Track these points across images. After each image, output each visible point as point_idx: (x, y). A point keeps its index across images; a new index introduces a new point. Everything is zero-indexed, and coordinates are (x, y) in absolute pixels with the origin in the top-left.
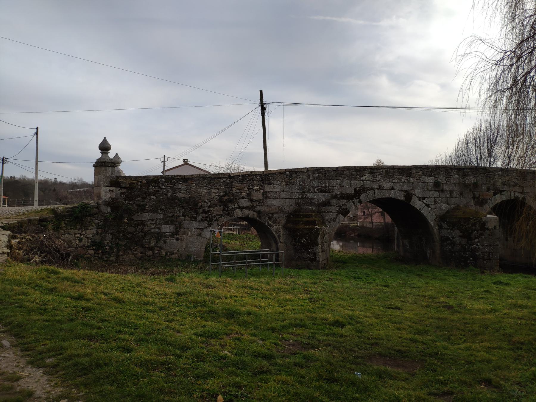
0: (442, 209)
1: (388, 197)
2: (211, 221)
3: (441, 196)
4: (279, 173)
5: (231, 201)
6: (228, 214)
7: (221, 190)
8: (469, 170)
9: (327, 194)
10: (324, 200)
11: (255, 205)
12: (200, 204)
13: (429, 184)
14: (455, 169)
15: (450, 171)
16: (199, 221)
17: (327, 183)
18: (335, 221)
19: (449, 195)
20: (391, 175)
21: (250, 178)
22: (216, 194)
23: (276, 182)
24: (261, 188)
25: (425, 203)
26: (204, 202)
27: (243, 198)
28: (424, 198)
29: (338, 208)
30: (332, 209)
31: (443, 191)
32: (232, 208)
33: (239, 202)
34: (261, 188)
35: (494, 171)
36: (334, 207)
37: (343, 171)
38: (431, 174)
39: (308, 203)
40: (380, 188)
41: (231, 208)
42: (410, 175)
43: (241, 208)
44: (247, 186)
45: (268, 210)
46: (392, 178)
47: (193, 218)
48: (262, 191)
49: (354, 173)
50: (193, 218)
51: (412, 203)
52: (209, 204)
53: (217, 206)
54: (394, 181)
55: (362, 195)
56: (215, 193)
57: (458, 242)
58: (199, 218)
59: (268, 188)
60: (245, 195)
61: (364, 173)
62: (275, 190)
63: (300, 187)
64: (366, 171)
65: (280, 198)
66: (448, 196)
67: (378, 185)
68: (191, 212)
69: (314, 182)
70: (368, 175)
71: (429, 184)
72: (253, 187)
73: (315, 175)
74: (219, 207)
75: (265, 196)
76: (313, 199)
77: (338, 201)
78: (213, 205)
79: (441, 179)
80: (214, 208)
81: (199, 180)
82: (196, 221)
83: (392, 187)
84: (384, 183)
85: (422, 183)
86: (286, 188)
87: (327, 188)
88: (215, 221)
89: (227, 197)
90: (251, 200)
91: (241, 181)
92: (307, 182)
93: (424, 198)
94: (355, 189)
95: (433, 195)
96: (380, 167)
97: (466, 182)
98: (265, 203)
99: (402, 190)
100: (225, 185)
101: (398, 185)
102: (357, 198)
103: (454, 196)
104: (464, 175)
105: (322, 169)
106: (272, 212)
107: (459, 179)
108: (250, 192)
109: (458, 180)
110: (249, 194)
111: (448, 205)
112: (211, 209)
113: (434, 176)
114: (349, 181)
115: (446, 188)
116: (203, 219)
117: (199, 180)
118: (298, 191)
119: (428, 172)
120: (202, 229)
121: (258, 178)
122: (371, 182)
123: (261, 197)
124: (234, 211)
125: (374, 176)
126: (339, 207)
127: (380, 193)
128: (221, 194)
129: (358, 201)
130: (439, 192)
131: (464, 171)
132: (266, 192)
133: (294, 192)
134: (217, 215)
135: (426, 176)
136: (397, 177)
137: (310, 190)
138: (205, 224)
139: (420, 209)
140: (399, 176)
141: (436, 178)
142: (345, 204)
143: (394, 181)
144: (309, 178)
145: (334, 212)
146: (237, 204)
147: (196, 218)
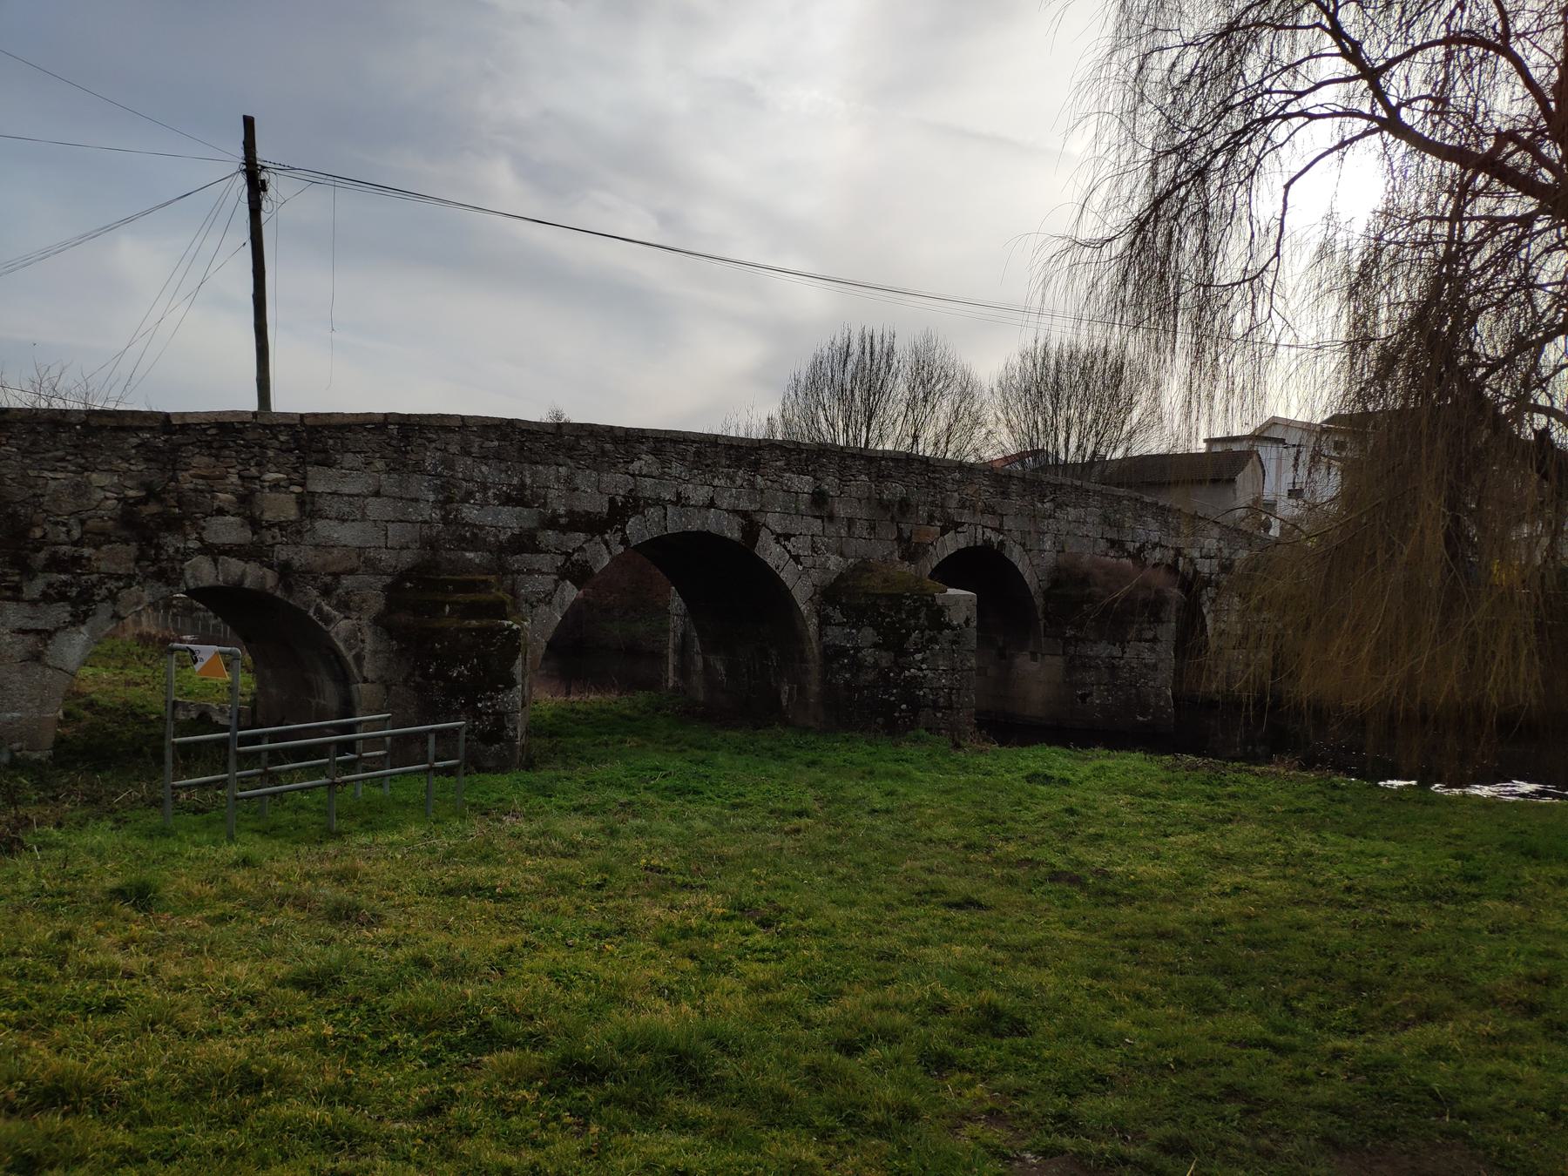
2: (85, 602)
3: (827, 532)
4: (362, 425)
5: (173, 525)
6: (161, 576)
7: (132, 478)
9: (526, 512)
10: (516, 531)
11: (269, 541)
12: (38, 533)
14: (863, 457)
16: (33, 603)
17: (527, 473)
18: (550, 602)
20: (709, 462)
21: (250, 436)
22: (109, 494)
24: (295, 476)
25: (789, 552)
26: (57, 523)
27: (221, 512)
28: (788, 537)
29: (560, 561)
30: (543, 561)
32: (177, 550)
33: (204, 528)
34: (295, 476)
35: (946, 468)
36: (548, 557)
37: (578, 437)
39: (464, 538)
40: (680, 501)
41: (171, 550)
42: (756, 467)
43: (213, 551)
44: (240, 467)
45: (319, 561)
47: (7, 588)
48: (297, 489)
49: (608, 446)
50: (7, 588)
52: (76, 533)
53: (111, 542)
54: (716, 482)
56: (102, 488)
58: (35, 588)
59: (320, 481)
60: (230, 502)
61: (635, 451)
62: (346, 490)
63: (438, 482)
64: (642, 443)
65: (364, 518)
66: (843, 532)
69: (484, 468)
70: (649, 458)
72: (262, 474)
73: (488, 444)
74: (118, 547)
75: (308, 507)
76: (481, 528)
77: (561, 535)
78: (100, 538)
79: (830, 484)
80: (97, 547)
83: (712, 498)
86: (389, 483)
87: (528, 492)
88: (103, 600)
89: (153, 508)
90: (255, 524)
91: (215, 445)
92: (462, 466)
94: (612, 501)
98: (307, 536)
99: (735, 512)
100: (147, 460)
101: (727, 494)
105: (512, 424)
106: (334, 569)
107: (870, 487)
108: (253, 492)
112: (87, 551)
114: (594, 474)
115: (841, 510)
116: (51, 591)
118: (432, 497)
119: (800, 460)
120: (46, 635)
123: (292, 513)
124: (182, 562)
125: (664, 463)
127: (681, 517)
128: (131, 493)
132: (313, 494)
133: (417, 500)
134: (111, 576)
137: (470, 494)
138: (62, 612)
140: (729, 467)
142: (581, 549)
143: (716, 482)
144: (469, 454)
145: (548, 574)
146: (195, 536)
147: (17, 589)
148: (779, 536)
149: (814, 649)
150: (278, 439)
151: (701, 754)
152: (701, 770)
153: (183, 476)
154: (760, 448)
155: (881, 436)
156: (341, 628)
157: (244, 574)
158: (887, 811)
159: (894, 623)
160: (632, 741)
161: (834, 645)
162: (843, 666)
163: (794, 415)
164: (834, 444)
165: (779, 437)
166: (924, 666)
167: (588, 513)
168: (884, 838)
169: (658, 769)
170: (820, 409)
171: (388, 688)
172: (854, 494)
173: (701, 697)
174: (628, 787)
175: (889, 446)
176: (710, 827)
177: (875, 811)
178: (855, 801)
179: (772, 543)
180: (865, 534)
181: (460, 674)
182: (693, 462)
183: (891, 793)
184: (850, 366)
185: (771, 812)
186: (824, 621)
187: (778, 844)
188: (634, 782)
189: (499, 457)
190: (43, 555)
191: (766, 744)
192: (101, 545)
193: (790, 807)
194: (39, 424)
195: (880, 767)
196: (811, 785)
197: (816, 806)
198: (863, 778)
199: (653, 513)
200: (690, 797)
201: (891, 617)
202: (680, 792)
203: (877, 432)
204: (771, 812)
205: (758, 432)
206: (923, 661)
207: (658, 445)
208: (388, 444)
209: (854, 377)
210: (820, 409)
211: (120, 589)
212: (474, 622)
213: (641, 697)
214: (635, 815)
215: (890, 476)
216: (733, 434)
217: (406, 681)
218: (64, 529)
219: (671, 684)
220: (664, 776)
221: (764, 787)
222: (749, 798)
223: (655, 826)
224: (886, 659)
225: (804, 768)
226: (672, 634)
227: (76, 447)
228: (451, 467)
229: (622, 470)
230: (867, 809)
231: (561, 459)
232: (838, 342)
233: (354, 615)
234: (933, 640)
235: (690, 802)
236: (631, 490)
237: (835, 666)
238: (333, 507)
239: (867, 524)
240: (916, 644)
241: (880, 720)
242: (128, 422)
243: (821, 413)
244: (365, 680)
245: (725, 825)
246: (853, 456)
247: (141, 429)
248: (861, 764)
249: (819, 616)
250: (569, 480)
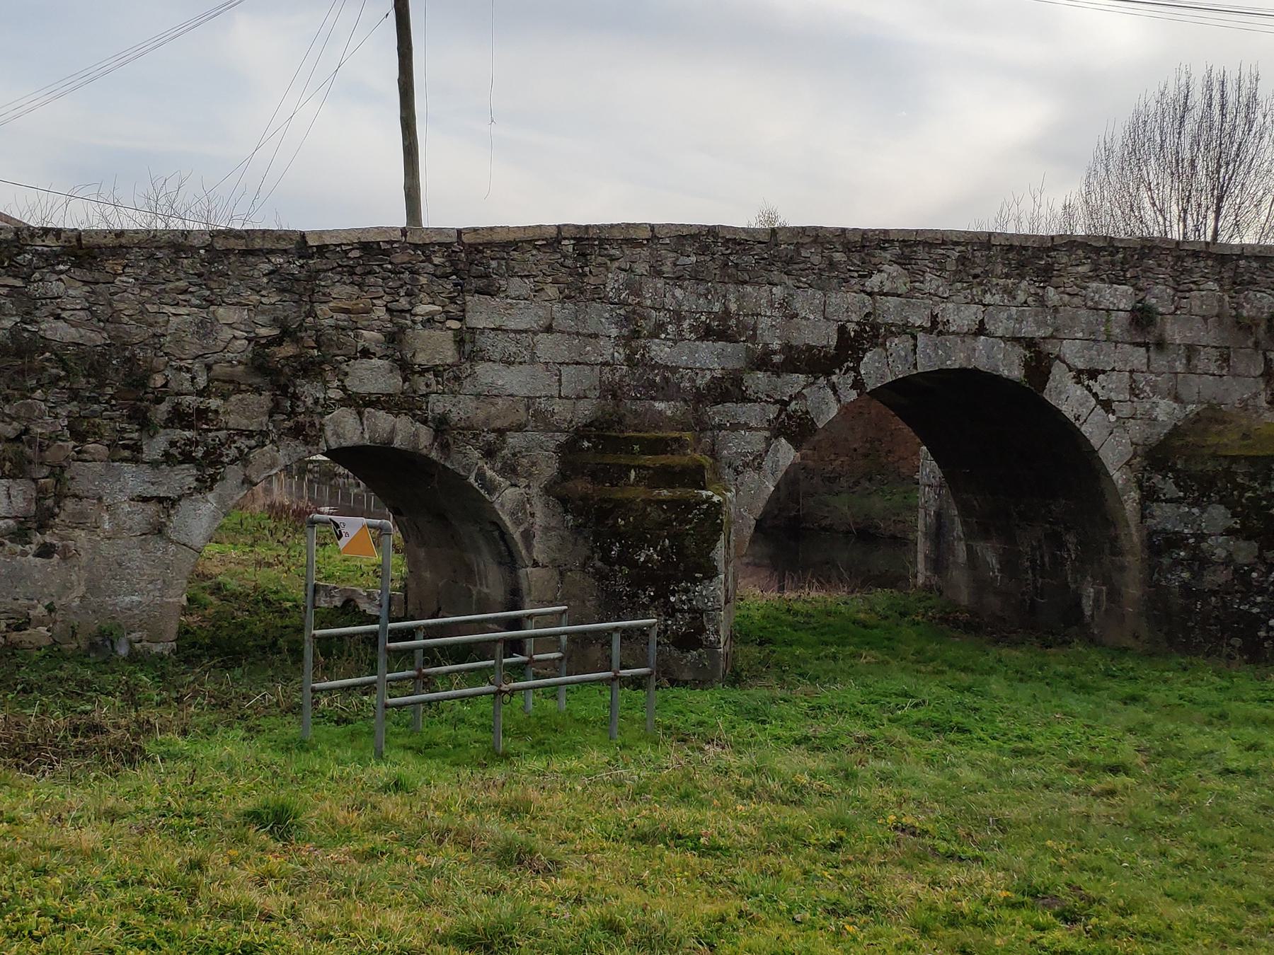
0: (1155, 419)
1: (965, 365)
2: (212, 464)
3: (1154, 366)
4: (530, 242)
5: (310, 369)
6: (297, 432)
7: (263, 313)
8: (1255, 264)
9: (730, 348)
10: (718, 374)
12: (159, 380)
13: (1114, 314)
14: (1209, 255)
15: (1189, 263)
16: (154, 464)
17: (731, 297)
18: (760, 467)
19: (1184, 361)
20: (978, 271)
21: (399, 258)
22: (238, 333)
23: (516, 286)
24: (452, 308)
25: (1095, 395)
26: (180, 369)
27: (366, 353)
28: (1093, 374)
29: (772, 412)
30: (750, 413)
31: (1161, 345)
32: (316, 401)
33: (346, 374)
34: (452, 308)
36: (757, 407)
37: (799, 246)
38: (1124, 276)
39: (652, 384)
40: (936, 326)
41: (310, 401)
42: (1046, 275)
43: (360, 403)
44: (387, 298)
45: (481, 415)
46: (980, 284)
47: (125, 447)
48: (455, 324)
49: (839, 256)
50: (125, 447)
51: (1049, 396)
52: (202, 381)
53: (240, 392)
54: (988, 298)
55: (868, 354)
56: (229, 325)
57: (1221, 553)
58: (155, 447)
59: (482, 313)
60: (378, 341)
61: (874, 260)
63: (622, 312)
64: (884, 249)
65: (533, 361)
66: (1179, 366)
67: (928, 312)
70: (894, 269)
71: (1114, 314)
72: (413, 305)
73: (683, 260)
74: (251, 397)
75: (468, 347)
76: (674, 370)
77: (774, 378)
78: (229, 386)
79: (1159, 297)
80: (225, 397)
82: (136, 461)
83: (982, 322)
84: (950, 305)
85: (1090, 308)
86: (562, 315)
87: (733, 322)
88: (232, 462)
89: (288, 349)
90: (405, 368)
92: (653, 287)
93: (1093, 374)
94: (842, 330)
95: (1126, 362)
96: (939, 236)
97: (1245, 313)
98: (466, 383)
99: (1016, 340)
100: (282, 291)
101: (1003, 315)
102: (848, 369)
103: (1201, 366)
104: (1239, 284)
105: (712, 231)
106: (498, 424)
107: (1221, 300)
108: (402, 329)
109: (1215, 304)
110: (394, 338)
111: (1175, 405)
112: (214, 403)
113: (1133, 281)
114: (819, 294)
115: (1176, 333)
116: (174, 451)
118: (614, 332)
119: (1113, 263)
120: (168, 503)
122: (904, 300)
123: (448, 354)
124: (322, 415)
125: (915, 275)
127: (936, 347)
128: (263, 331)
129: (850, 381)
130: (1148, 351)
131: (1238, 266)
132: (473, 330)
133: (596, 336)
134: (241, 433)
135: (1103, 280)
136: (1001, 282)
137: (661, 326)
138: (185, 476)
139: (1077, 419)
140: (1007, 276)
141: (1141, 290)
142: (799, 396)
143: (988, 298)
144: (659, 274)
145: (757, 429)
146: (336, 383)
147: (136, 448)
148: (1080, 372)
149: (1133, 536)
150: (431, 262)
151: (967, 679)
152: (968, 699)
153: (321, 309)
154: (1054, 248)
155: (1237, 224)
156: (506, 498)
157: (393, 431)
158: (1248, 773)
159: (1260, 499)
160: (869, 656)
161: (1164, 530)
162: (1178, 562)
163: (1103, 199)
164: (1164, 240)
165: (1080, 231)
167: (810, 348)
168: (1244, 810)
169: (906, 695)
170: (1142, 188)
172: (1196, 310)
173: (964, 598)
174: (866, 717)
175: (1249, 238)
176: (983, 779)
177: (1229, 771)
178: (1199, 756)
179: (1070, 383)
180: (1213, 368)
181: (649, 559)
182: (957, 272)
183: (1253, 747)
184: (1190, 126)
185: (1072, 764)
187: (1083, 808)
188: (874, 711)
189: (697, 278)
190: (164, 407)
191: (1061, 669)
192: (230, 395)
193: (1100, 758)
194: (158, 248)
195: (1236, 708)
196: (1130, 730)
197: (1140, 759)
198: (1210, 724)
199: (898, 345)
200: (952, 736)
201: (1254, 490)
202: (939, 728)
203: (1231, 219)
204: (1072, 764)
205: (1049, 226)
207: (907, 251)
208: (562, 265)
209: (1196, 141)
210: (1142, 188)
212: (665, 493)
213: (881, 597)
214: (878, 756)
215: (1253, 282)
216: (1011, 230)
217: (584, 566)
218: (188, 376)
219: (920, 580)
220: (916, 705)
221: (1061, 729)
222: (1039, 743)
223: (905, 773)
225: (1119, 706)
226: (922, 511)
227: (200, 275)
228: (637, 293)
229: (856, 288)
230: (1217, 767)
231: (776, 276)
232: (1171, 91)
233: (523, 482)
235: (953, 743)
236: (868, 314)
237: (1166, 561)
238: (496, 345)
239: (1216, 353)
241: (1237, 642)
242: (258, 244)
243: (1144, 195)
244: (536, 564)
245: (1004, 778)
246: (1195, 254)
247: (272, 252)
248: (1206, 703)
249: (1140, 487)
250: (785, 304)
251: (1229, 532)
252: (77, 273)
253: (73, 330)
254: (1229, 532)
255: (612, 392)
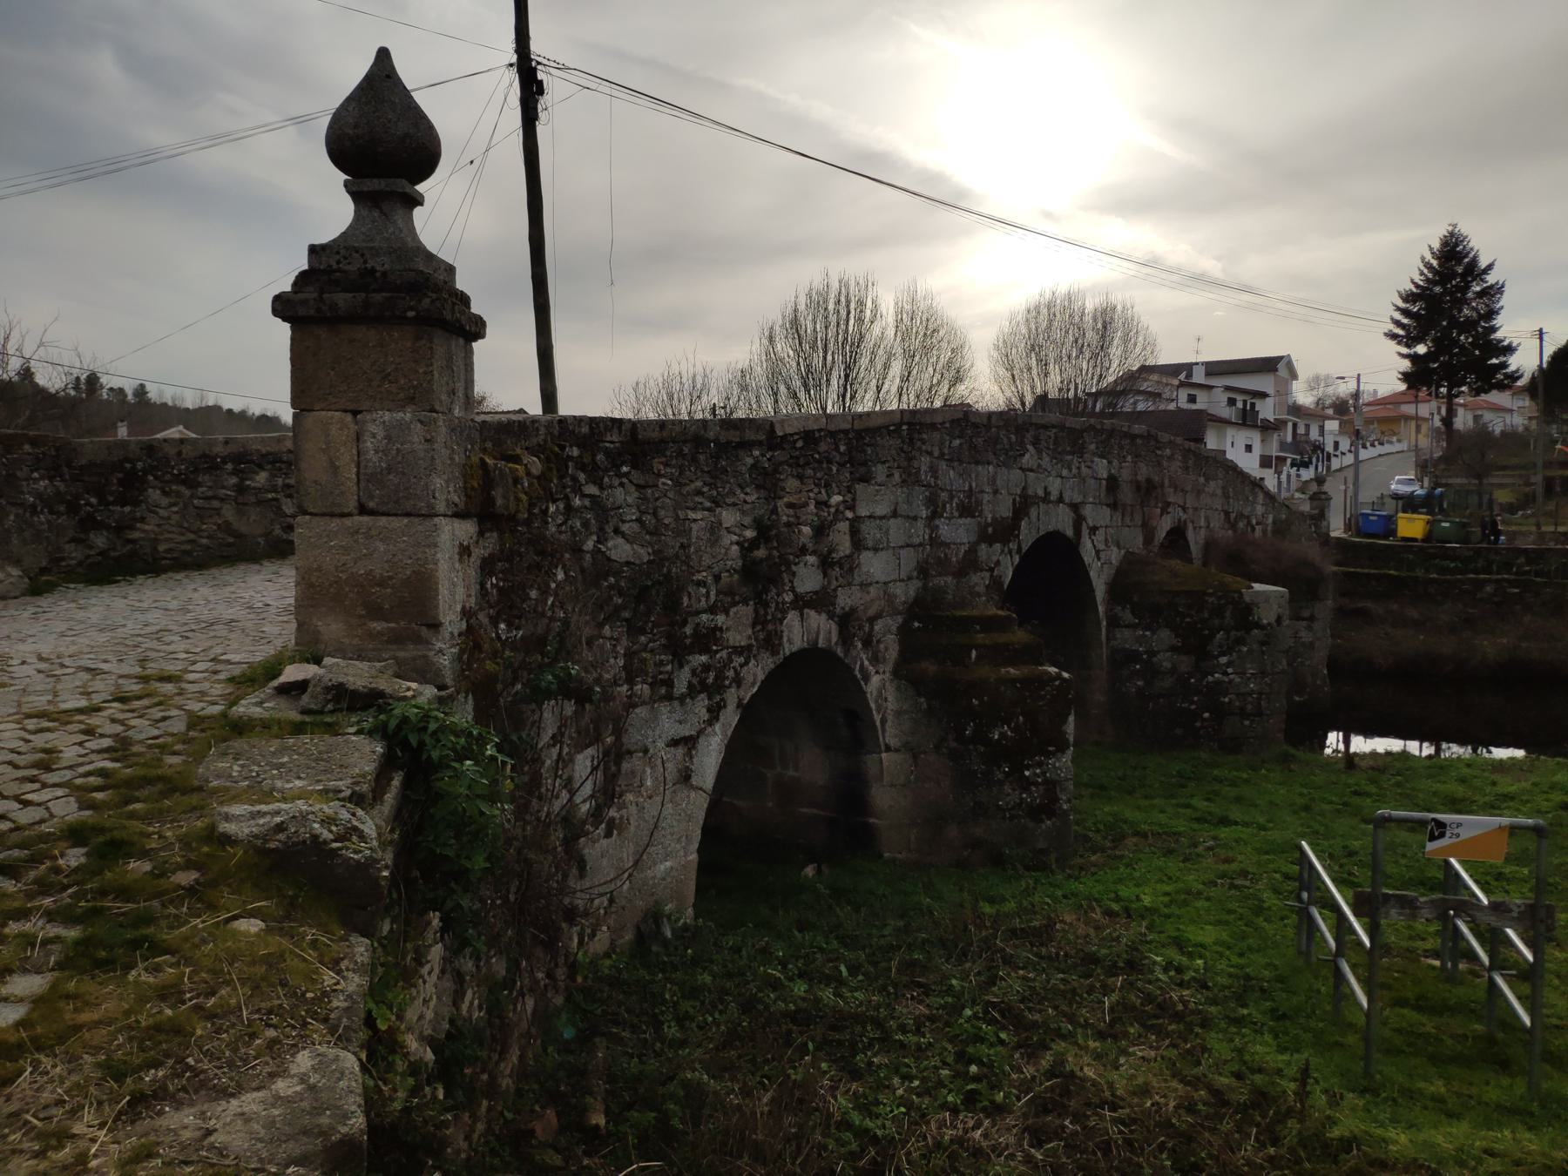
16: (682, 699)
27: (803, 551)
44: (816, 490)
57: (1167, 665)
65: (888, 548)
68: (652, 651)
72: (829, 496)
80: (727, 612)
81: (680, 454)
82: (669, 697)
91: (802, 461)
100: (758, 487)
110: (820, 531)
116: (695, 681)
117: (680, 454)
120: (689, 743)
121: (842, 448)
126: (988, 574)
138: (701, 705)
153: (780, 503)
166: (1230, 670)
171: (915, 757)
181: (1003, 735)
186: (1114, 622)
190: (688, 630)
194: (685, 442)
206: (1229, 664)
211: (742, 666)
212: (1012, 670)
224: (1185, 663)
234: (1240, 641)
238: (870, 532)
240: (1220, 646)
242: (750, 435)
244: (888, 749)
251: (1173, 649)
252: (635, 475)
253: (628, 547)
254: (1173, 649)
255: (923, 571)
